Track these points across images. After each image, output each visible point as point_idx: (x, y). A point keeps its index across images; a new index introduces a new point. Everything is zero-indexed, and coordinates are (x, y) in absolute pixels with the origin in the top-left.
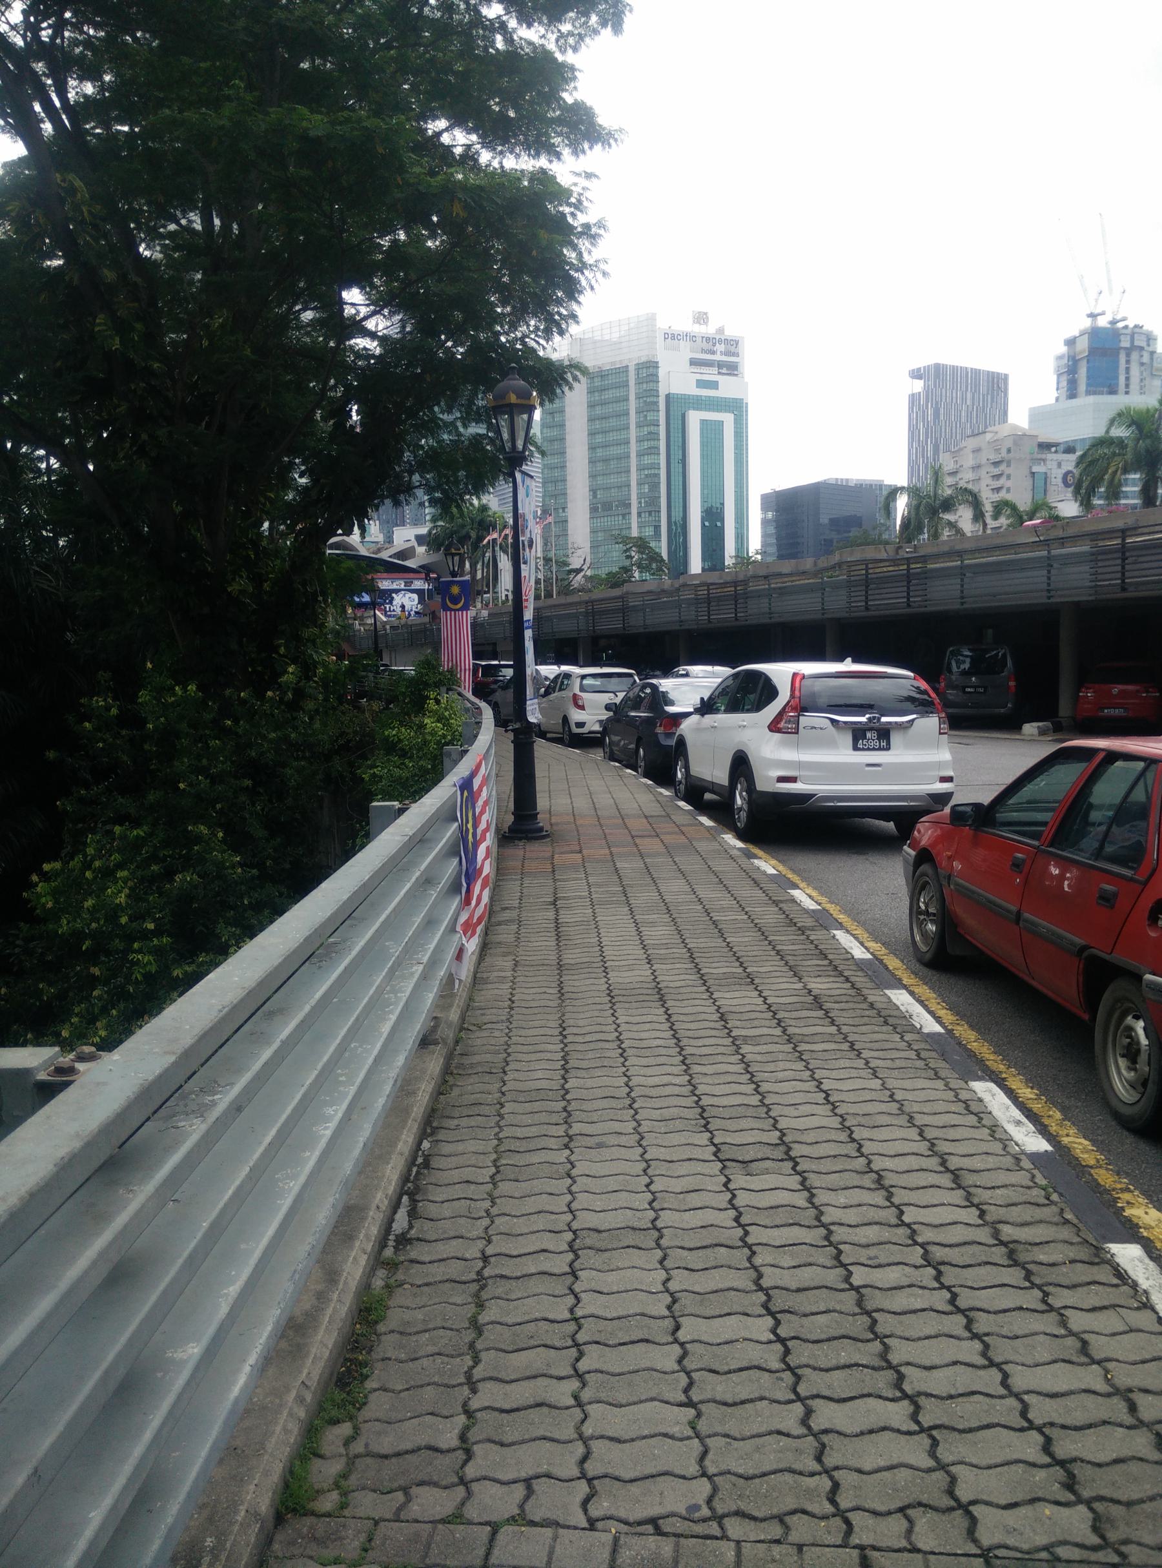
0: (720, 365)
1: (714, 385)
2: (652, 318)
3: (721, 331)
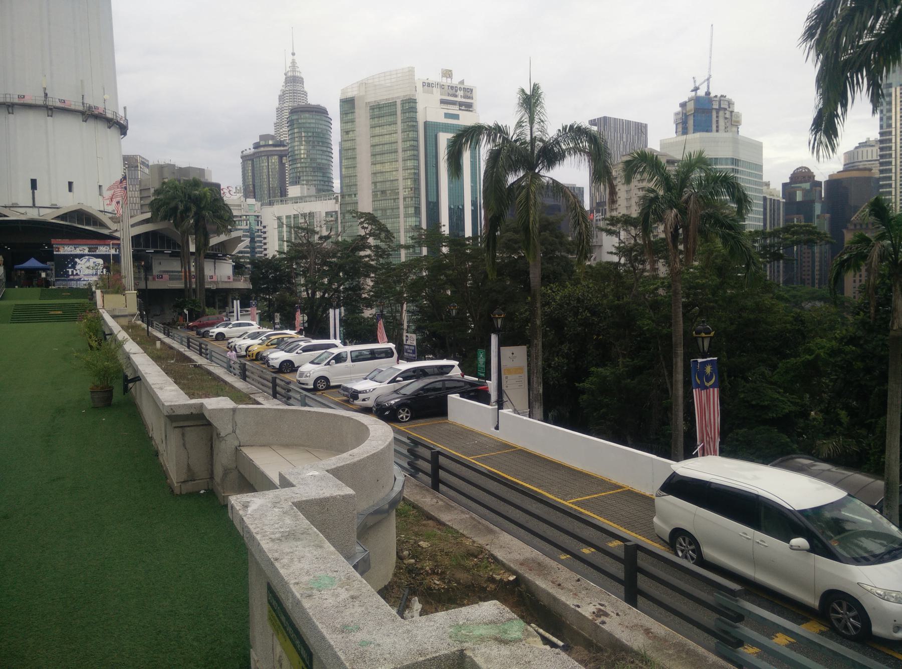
0: (461, 104)
1: (456, 117)
2: (411, 71)
3: (462, 82)
